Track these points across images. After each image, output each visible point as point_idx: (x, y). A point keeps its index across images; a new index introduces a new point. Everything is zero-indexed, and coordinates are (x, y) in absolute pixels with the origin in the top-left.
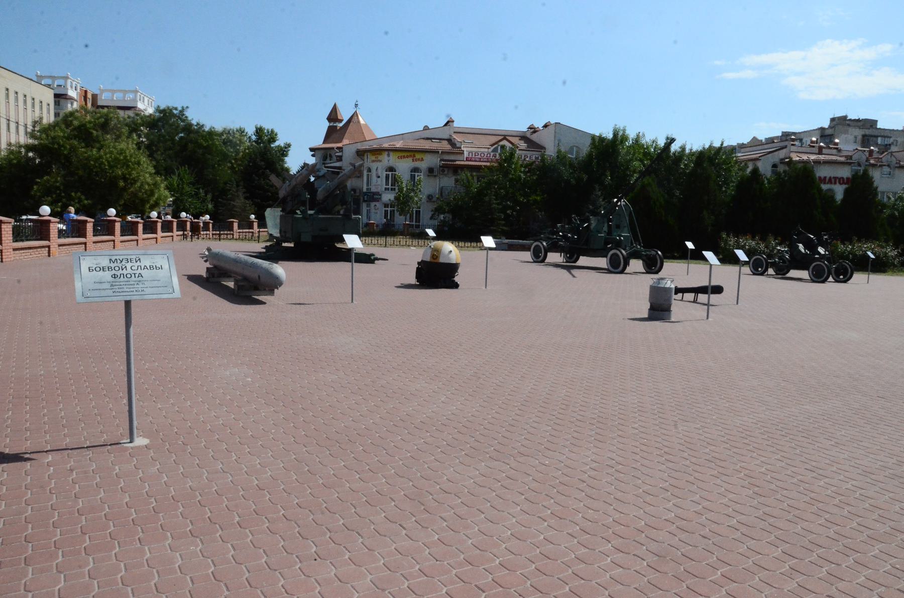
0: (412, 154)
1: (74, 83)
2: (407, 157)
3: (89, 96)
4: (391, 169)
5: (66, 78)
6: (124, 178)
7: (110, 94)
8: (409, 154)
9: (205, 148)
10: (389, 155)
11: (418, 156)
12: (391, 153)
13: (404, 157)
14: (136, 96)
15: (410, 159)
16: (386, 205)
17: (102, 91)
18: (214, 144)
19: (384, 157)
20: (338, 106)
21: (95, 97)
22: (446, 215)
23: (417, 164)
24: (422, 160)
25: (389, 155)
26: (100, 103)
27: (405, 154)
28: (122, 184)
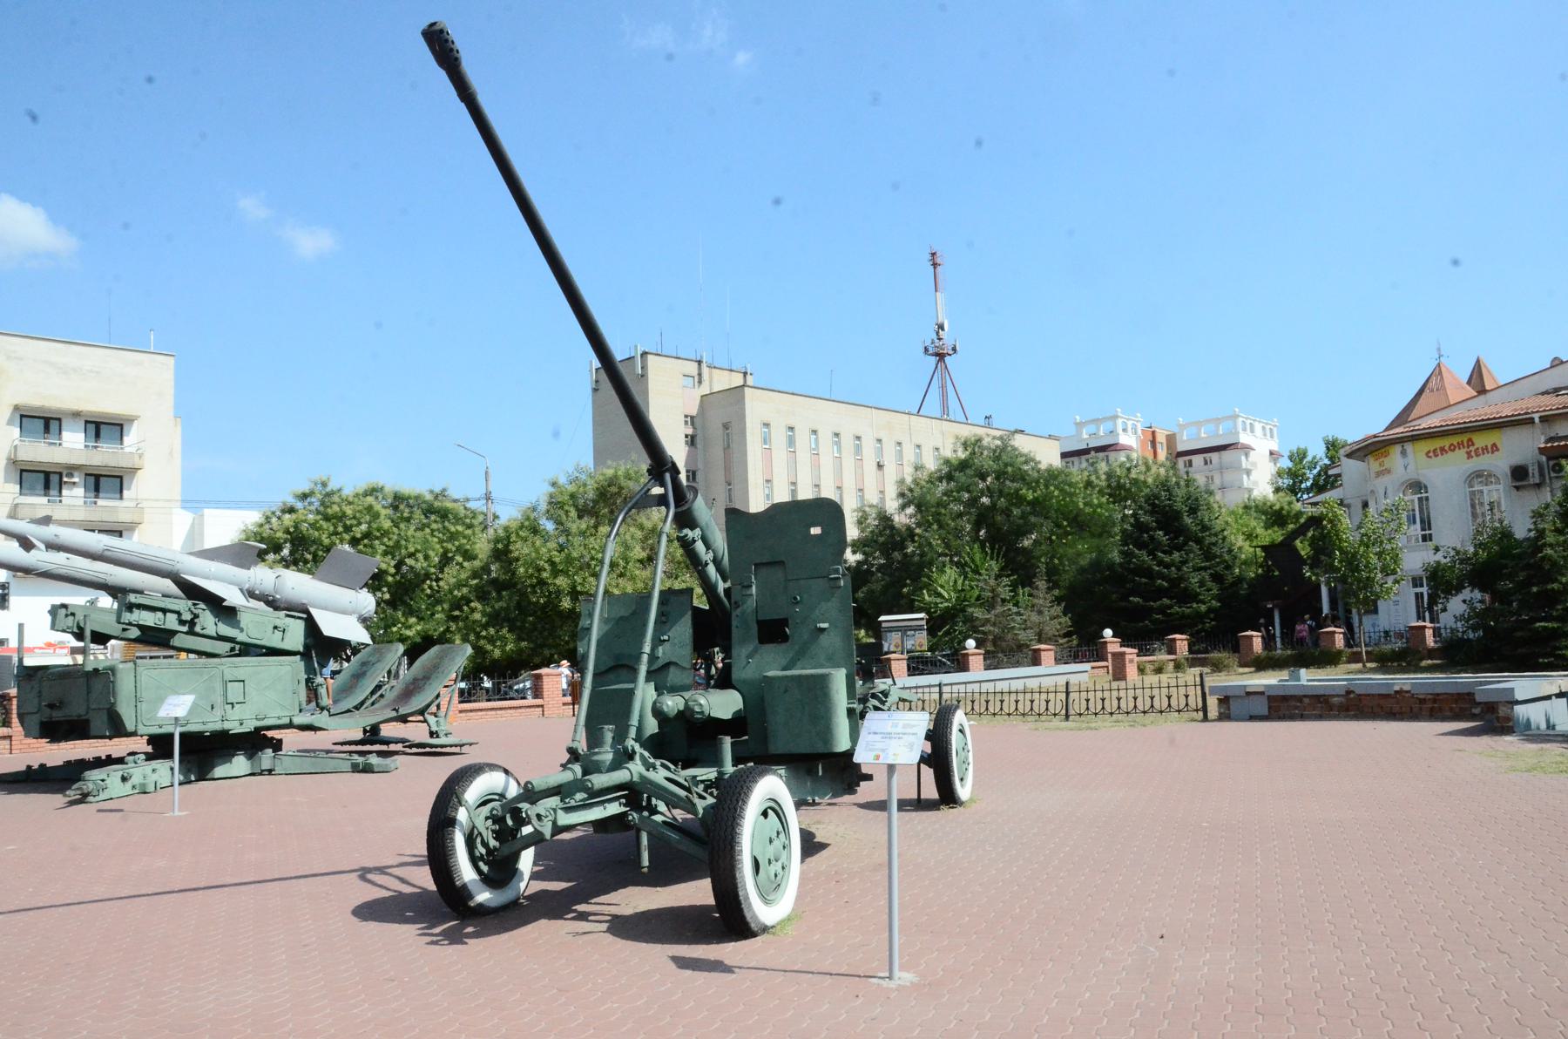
0: (1465, 438)
1: (1130, 423)
2: (1452, 448)
3: (1161, 438)
4: (1417, 486)
5: (1115, 417)
6: (574, 594)
7: (1211, 427)
8: (1455, 440)
9: (1035, 503)
10: (1404, 453)
11: (1481, 440)
12: (1409, 447)
13: (1443, 450)
14: (1235, 426)
15: (1461, 453)
16: (1416, 582)
17: (1182, 427)
18: (1049, 496)
19: (1395, 457)
20: (1485, 361)
21: (1171, 439)
22: (1466, 593)
23: (1484, 462)
24: (1495, 448)
25: (1404, 453)
26: (1180, 448)
27: (1446, 442)
28: (566, 603)
